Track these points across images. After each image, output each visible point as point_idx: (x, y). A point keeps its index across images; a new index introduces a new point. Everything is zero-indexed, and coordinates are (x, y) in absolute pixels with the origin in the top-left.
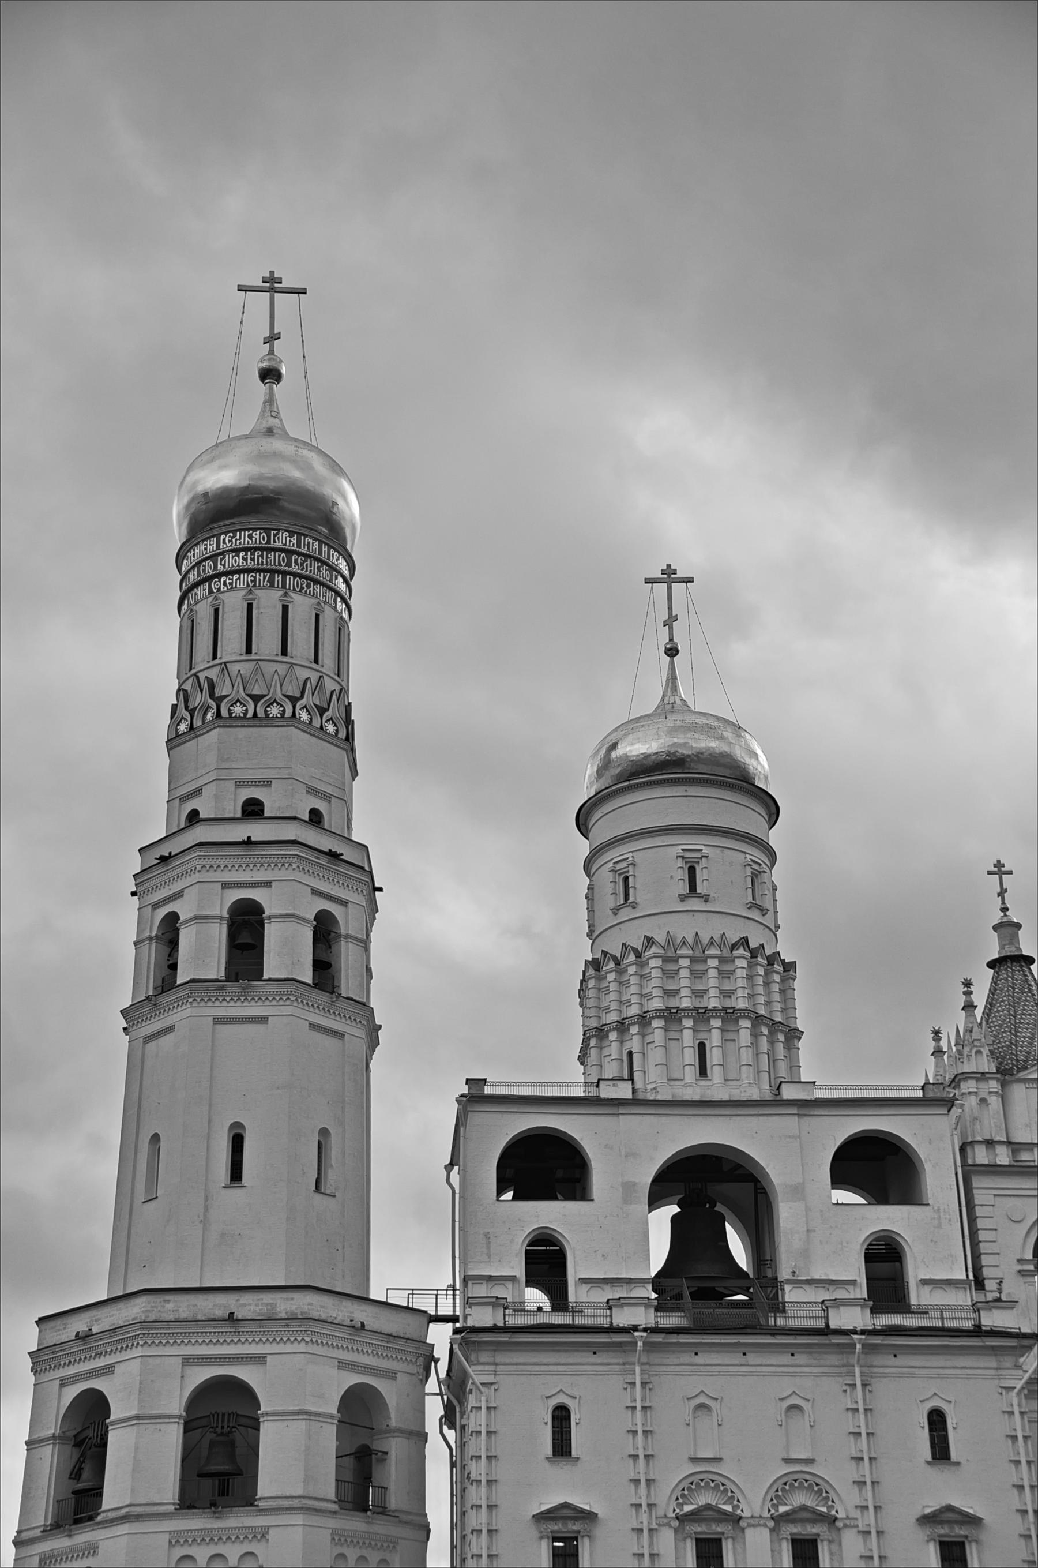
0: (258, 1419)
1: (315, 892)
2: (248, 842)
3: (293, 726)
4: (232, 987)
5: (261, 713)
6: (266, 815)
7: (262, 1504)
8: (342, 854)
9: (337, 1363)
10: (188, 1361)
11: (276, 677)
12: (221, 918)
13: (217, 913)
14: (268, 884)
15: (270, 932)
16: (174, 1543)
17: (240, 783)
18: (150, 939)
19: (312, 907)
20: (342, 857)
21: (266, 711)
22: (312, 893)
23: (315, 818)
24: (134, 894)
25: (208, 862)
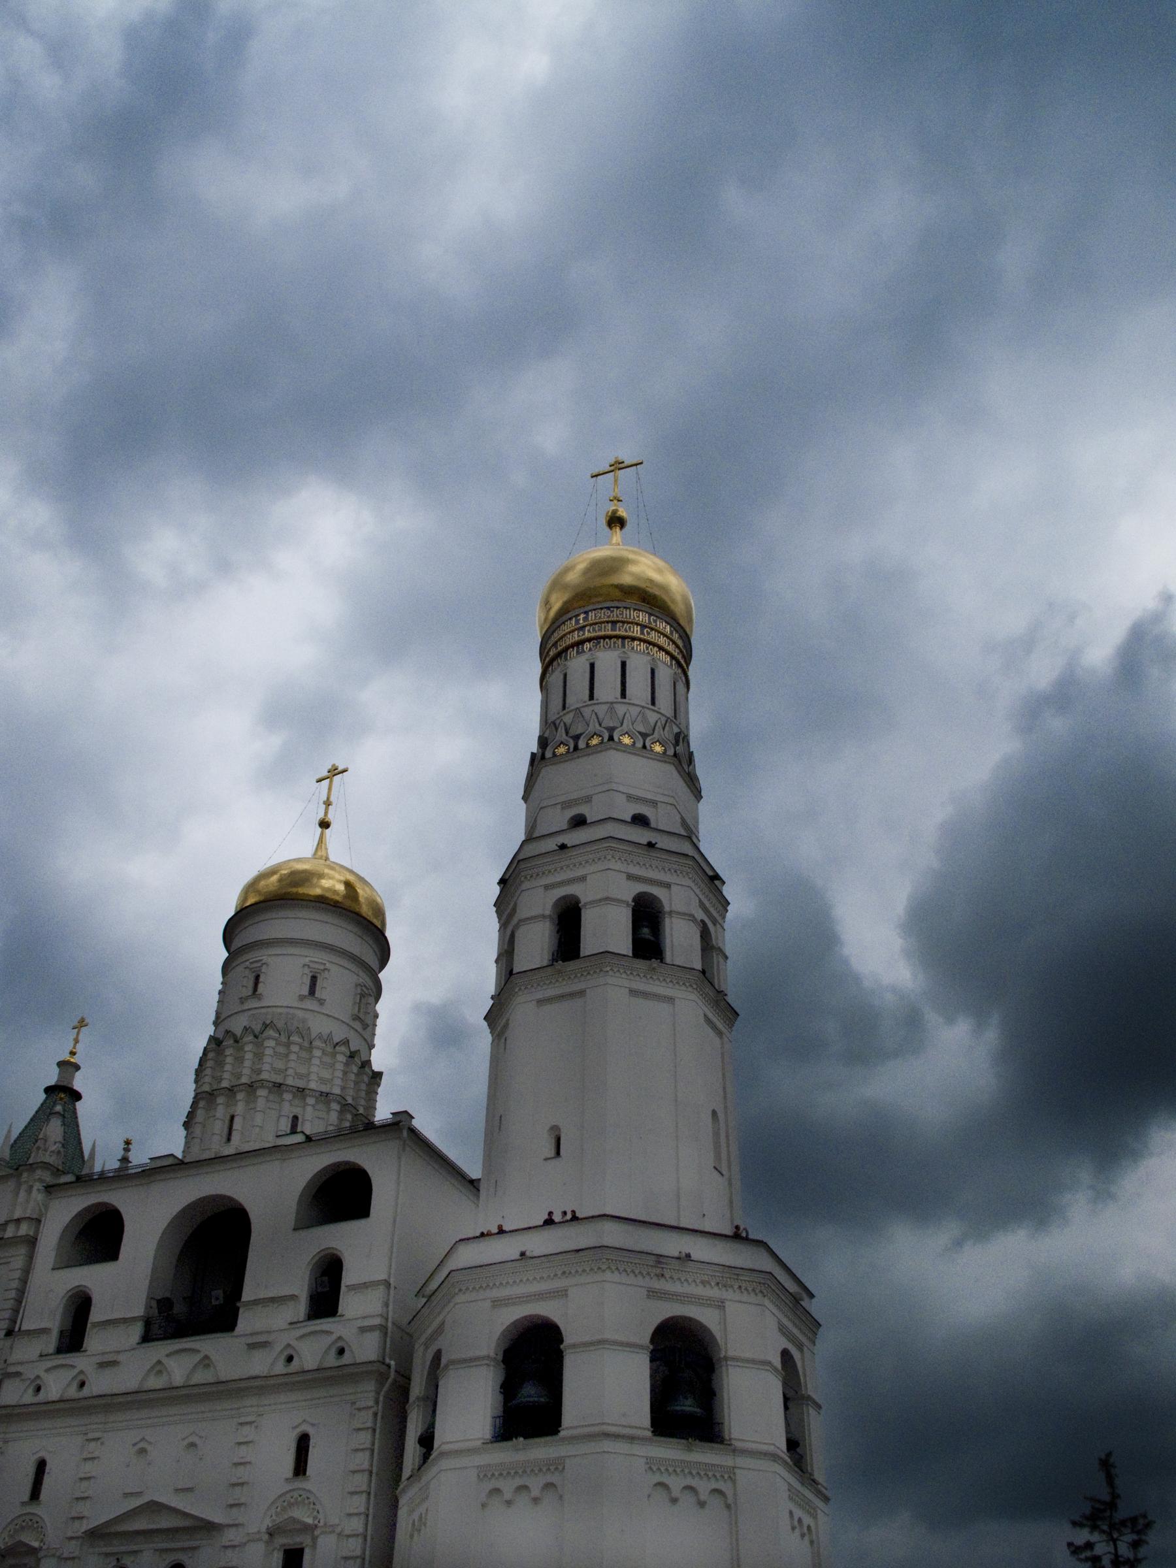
0: (562, 1352)
1: (630, 877)
2: (563, 847)
3: (611, 748)
5: (581, 744)
6: (588, 822)
7: (562, 1434)
8: (656, 843)
9: (646, 1293)
12: (544, 916)
13: (541, 912)
14: (583, 879)
15: (589, 919)
16: (481, 1477)
17: (566, 805)
19: (629, 891)
20: (657, 846)
22: (627, 879)
23: (640, 820)
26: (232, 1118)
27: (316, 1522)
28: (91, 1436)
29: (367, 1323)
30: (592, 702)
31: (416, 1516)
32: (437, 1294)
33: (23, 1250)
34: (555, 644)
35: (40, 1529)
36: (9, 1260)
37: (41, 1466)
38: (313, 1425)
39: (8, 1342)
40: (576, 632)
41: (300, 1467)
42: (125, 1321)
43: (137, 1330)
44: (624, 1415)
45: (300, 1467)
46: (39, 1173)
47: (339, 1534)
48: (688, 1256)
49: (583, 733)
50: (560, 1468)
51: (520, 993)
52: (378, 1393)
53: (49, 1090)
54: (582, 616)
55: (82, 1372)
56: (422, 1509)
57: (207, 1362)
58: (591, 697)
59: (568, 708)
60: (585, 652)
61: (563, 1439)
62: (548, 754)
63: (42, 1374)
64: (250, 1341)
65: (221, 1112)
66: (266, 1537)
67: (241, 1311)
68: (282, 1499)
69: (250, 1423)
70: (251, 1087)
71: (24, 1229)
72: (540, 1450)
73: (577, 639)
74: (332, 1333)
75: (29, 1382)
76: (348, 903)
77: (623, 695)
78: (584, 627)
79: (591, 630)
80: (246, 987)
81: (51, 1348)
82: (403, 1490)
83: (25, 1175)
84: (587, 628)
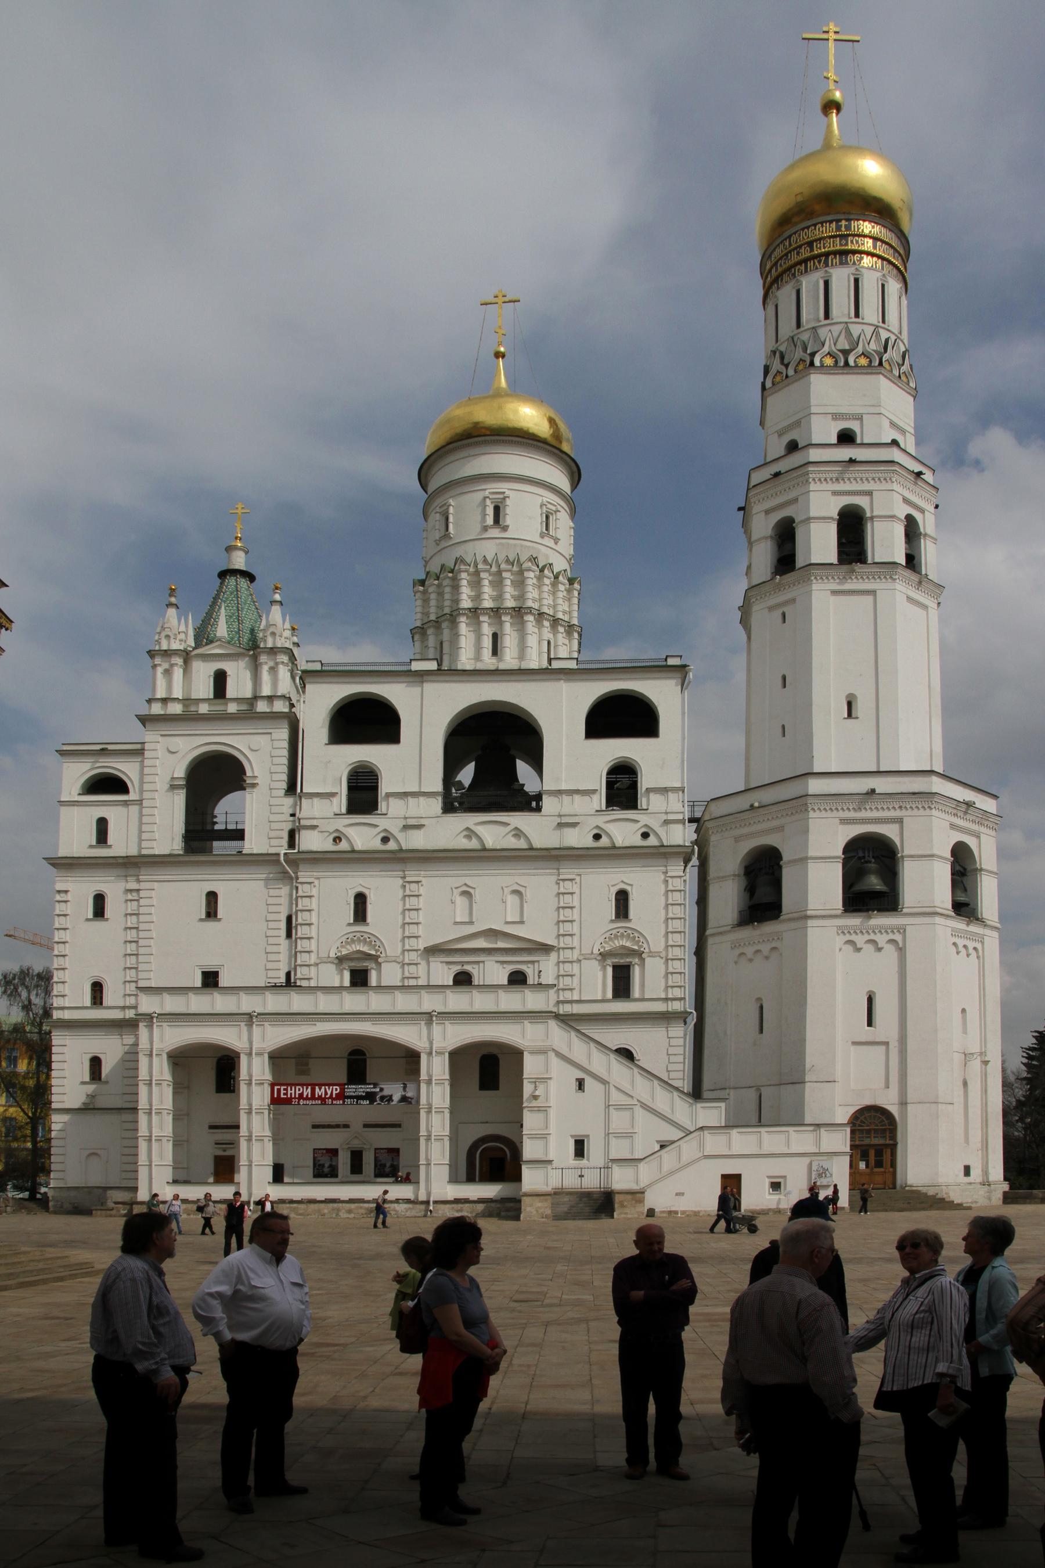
5: (851, 363)
6: (859, 441)
11: (862, 334)
17: (836, 417)
18: (765, 538)
21: (855, 362)
29: (671, 817)
30: (857, 320)
34: (810, 244)
40: (838, 239)
44: (943, 902)
48: (974, 803)
49: (851, 351)
54: (843, 223)
56: (765, 948)
58: (857, 315)
59: (832, 319)
60: (848, 264)
62: (817, 363)
69: (571, 880)
73: (838, 248)
74: (638, 821)
76: (554, 442)
77: (884, 322)
78: (849, 235)
79: (854, 242)
84: (850, 238)
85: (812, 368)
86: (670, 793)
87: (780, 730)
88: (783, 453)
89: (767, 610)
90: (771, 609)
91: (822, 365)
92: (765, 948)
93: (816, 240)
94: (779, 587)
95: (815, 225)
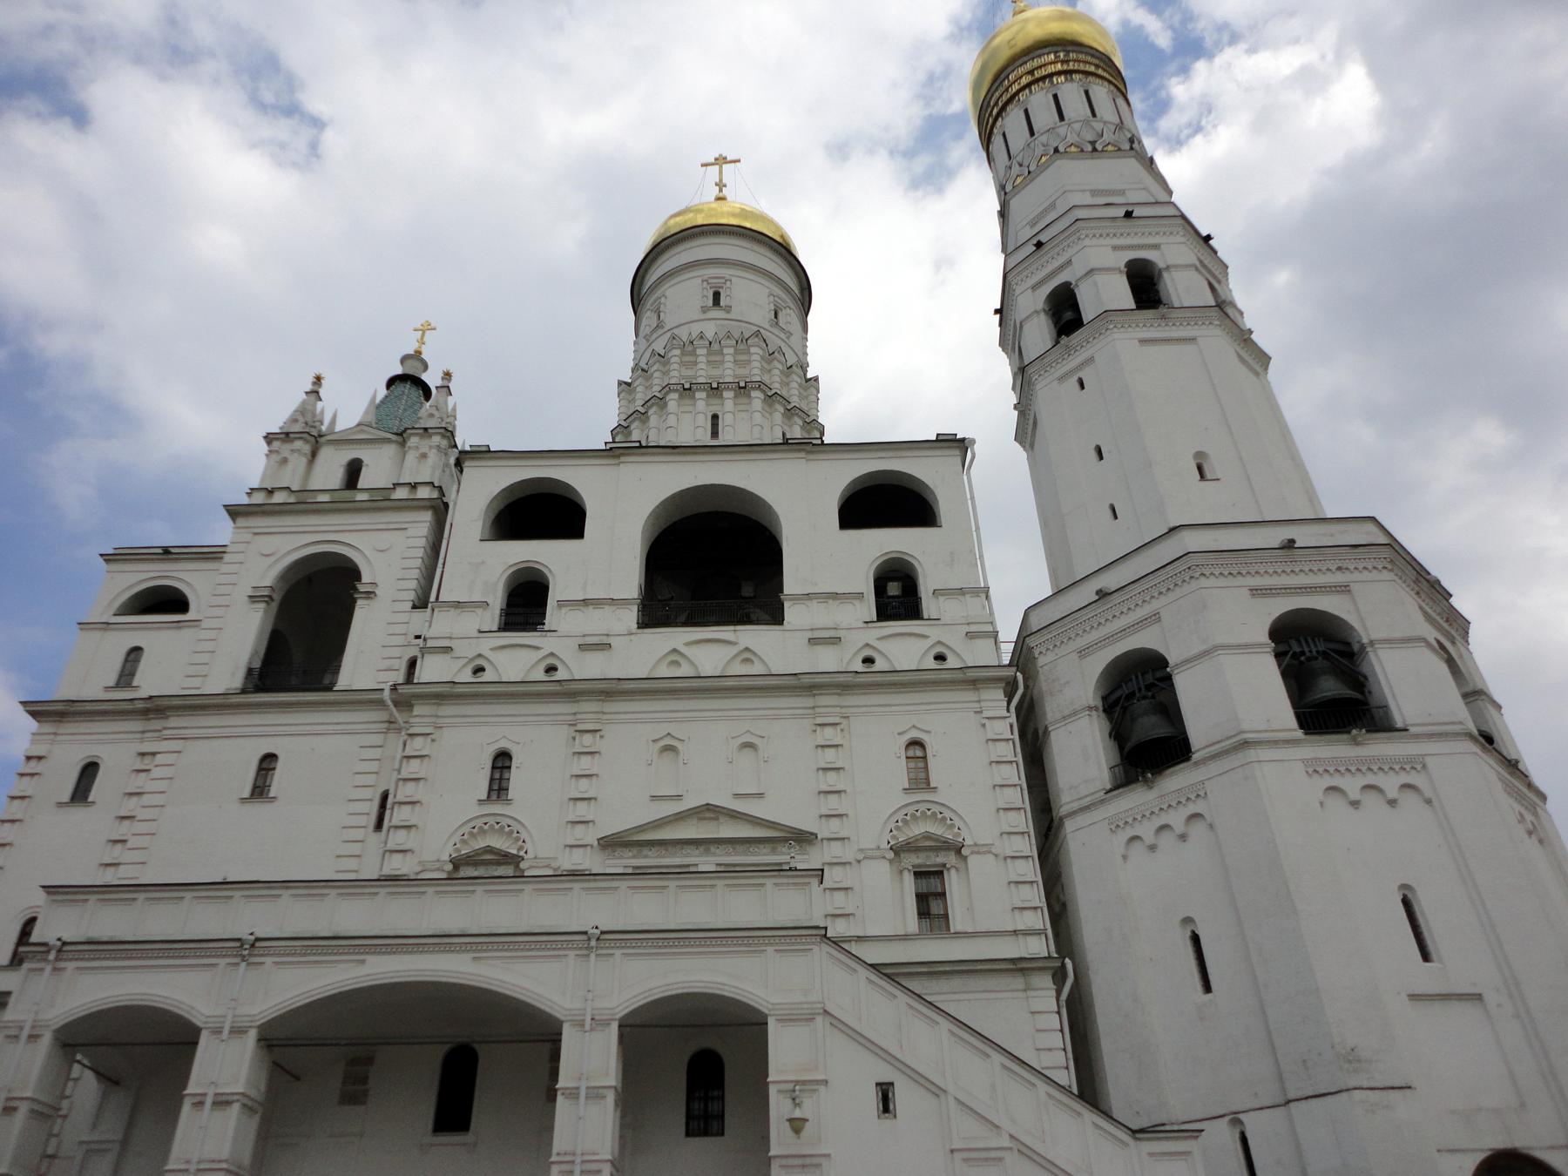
4: (1148, 314)
5: (1099, 147)
10: (1256, 592)
14: (1156, 247)
18: (1037, 312)
24: (997, 311)
25: (1098, 232)
26: (715, 417)
27: (961, 840)
28: (580, 727)
29: (973, 628)
31: (1146, 830)
32: (1127, 589)
33: (427, 516)
35: (515, 835)
36: (404, 526)
37: (502, 761)
38: (929, 732)
39: (421, 616)
41: (920, 780)
42: (613, 601)
43: (631, 616)
45: (920, 780)
46: (436, 439)
47: (996, 856)
50: (1419, 767)
51: (1115, 330)
52: (1009, 703)
53: (391, 382)
55: (552, 654)
56: (1176, 819)
57: (747, 655)
58: (1094, 114)
61: (1417, 736)
63: (487, 653)
64: (810, 635)
65: (701, 405)
66: (891, 855)
67: (786, 605)
68: (904, 811)
70: (742, 389)
71: (424, 493)
72: (1378, 747)
75: (466, 660)
80: (707, 297)
81: (495, 628)
82: (1073, 814)
83: (413, 441)
85: (1057, 154)
86: (967, 596)
87: (1109, 513)
88: (1057, 201)
89: (1057, 382)
90: (1062, 379)
91: (1066, 152)
92: (1176, 819)
93: (1037, 68)
94: (1069, 350)
95: (1033, 59)
